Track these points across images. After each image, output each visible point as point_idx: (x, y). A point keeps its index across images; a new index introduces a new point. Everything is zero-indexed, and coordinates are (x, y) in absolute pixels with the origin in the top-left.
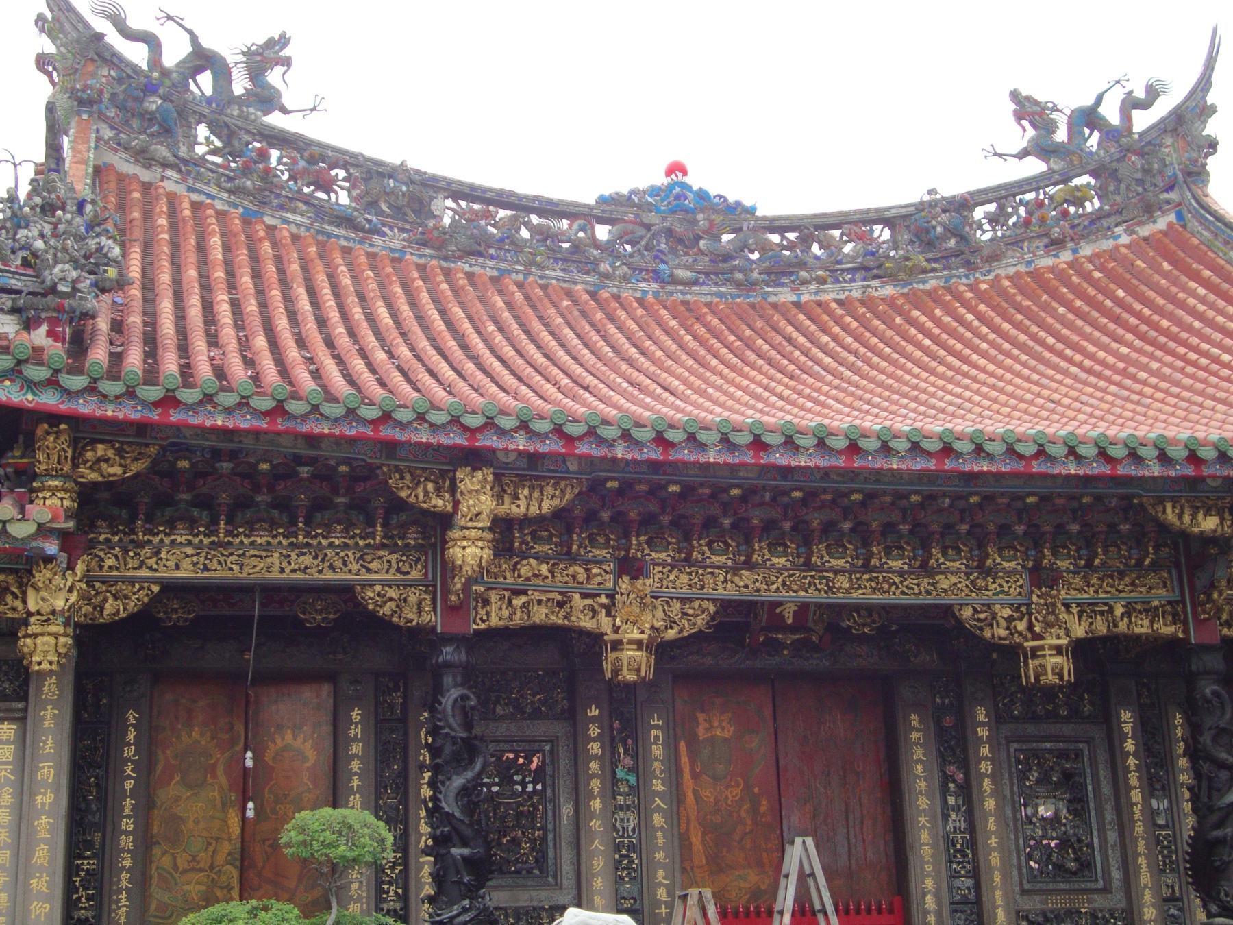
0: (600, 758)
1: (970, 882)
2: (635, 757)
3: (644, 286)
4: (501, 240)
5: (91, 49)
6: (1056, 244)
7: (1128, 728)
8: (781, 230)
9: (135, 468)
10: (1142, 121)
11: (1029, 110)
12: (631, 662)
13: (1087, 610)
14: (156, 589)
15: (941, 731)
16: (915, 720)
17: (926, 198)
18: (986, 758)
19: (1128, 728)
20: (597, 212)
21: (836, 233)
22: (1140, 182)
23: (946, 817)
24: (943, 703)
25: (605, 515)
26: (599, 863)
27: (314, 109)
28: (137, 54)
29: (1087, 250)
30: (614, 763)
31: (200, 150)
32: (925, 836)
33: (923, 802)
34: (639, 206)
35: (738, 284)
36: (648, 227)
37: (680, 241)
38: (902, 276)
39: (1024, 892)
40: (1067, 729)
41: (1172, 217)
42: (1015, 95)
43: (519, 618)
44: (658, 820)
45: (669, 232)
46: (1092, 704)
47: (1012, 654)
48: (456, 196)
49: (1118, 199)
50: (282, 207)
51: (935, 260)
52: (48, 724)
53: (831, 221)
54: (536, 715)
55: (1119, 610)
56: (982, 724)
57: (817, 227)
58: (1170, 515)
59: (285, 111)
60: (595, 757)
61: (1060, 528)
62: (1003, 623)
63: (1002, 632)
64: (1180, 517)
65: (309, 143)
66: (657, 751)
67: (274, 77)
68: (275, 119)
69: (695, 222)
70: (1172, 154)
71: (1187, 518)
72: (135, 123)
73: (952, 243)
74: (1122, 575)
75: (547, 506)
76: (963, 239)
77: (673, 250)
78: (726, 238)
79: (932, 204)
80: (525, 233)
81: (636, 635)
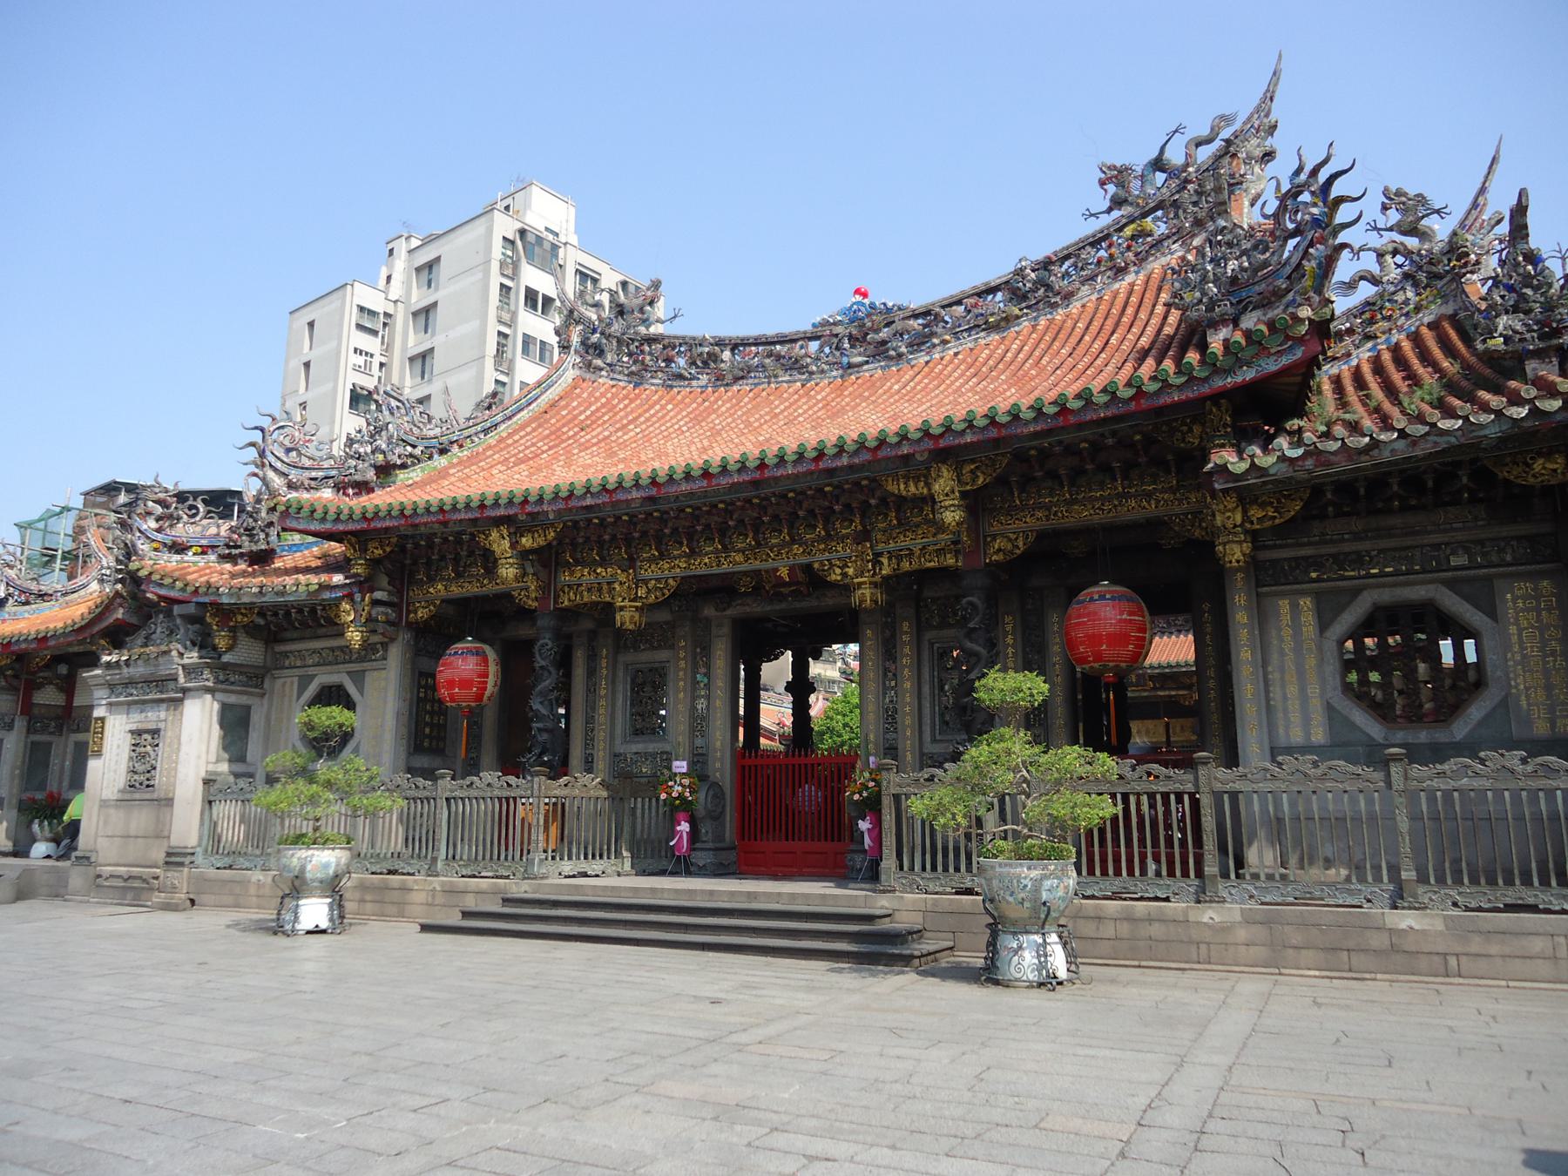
0: (685, 670)
2: (708, 668)
6: (1120, 271)
7: (1009, 628)
10: (1205, 154)
11: (1116, 176)
12: (627, 617)
13: (896, 556)
19: (1009, 628)
23: (885, 694)
30: (694, 673)
39: (934, 741)
44: (718, 703)
54: (659, 647)
57: (943, 307)
58: (892, 487)
62: (838, 571)
68: (655, 329)
74: (917, 526)
75: (541, 542)
76: (1048, 287)
81: (626, 603)
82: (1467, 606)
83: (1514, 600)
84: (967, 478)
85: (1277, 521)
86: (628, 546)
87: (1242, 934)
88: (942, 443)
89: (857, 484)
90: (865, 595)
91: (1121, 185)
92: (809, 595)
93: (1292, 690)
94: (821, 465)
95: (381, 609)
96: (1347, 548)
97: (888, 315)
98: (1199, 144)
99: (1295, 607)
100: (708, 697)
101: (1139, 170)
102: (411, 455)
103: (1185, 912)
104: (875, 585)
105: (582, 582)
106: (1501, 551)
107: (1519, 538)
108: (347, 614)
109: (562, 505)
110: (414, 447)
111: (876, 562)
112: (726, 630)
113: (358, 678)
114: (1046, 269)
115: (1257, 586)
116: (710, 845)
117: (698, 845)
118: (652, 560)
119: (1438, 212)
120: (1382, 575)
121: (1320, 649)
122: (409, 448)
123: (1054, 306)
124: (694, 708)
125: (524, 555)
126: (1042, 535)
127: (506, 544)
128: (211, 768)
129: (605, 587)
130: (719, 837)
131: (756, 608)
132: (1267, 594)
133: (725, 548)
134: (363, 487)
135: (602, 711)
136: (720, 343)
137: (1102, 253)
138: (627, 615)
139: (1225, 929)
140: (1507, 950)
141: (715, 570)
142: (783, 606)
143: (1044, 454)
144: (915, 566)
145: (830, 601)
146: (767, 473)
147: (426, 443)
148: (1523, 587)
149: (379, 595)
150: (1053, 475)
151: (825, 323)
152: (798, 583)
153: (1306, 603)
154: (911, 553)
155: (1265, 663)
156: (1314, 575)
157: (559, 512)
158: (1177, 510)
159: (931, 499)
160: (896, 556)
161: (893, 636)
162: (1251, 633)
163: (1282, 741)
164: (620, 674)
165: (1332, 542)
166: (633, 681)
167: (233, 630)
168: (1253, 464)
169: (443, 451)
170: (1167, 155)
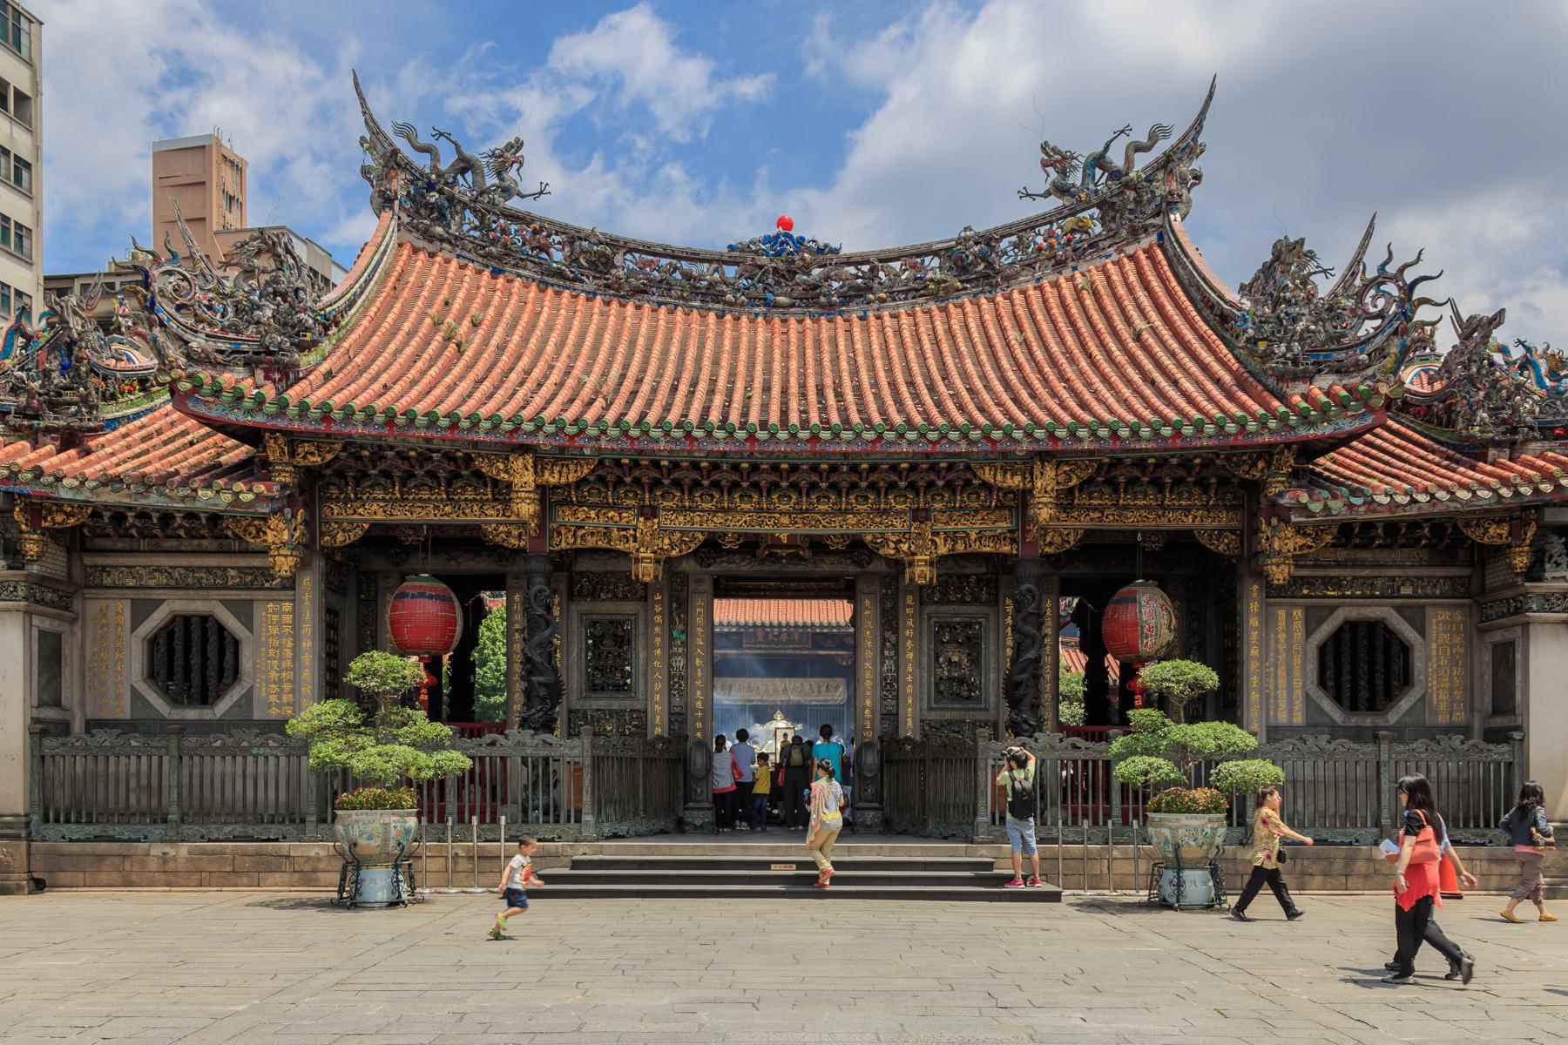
4: (661, 281)
8: (856, 264)
10: (1142, 161)
11: (1056, 160)
12: (646, 570)
13: (952, 537)
15: (884, 613)
16: (867, 602)
19: (1010, 609)
21: (896, 265)
22: (1131, 211)
23: (882, 664)
25: (628, 480)
27: (541, 193)
31: (466, 227)
32: (868, 675)
33: (869, 654)
34: (756, 252)
35: (822, 306)
36: (761, 267)
39: (930, 709)
40: (973, 609)
41: (1154, 238)
42: (1043, 149)
43: (578, 545)
46: (989, 594)
47: (898, 566)
48: (630, 251)
49: (1113, 226)
50: (516, 265)
52: (307, 603)
55: (973, 537)
57: (881, 261)
59: (523, 197)
61: (931, 484)
68: (514, 204)
69: (793, 262)
72: (422, 211)
73: (981, 267)
74: (977, 511)
76: (990, 265)
77: (778, 283)
78: (816, 272)
79: (966, 239)
80: (678, 275)
81: (649, 554)
90: (922, 572)
91: (1063, 173)
96: (1333, 572)
98: (1139, 148)
99: (1289, 615)
103: (1235, 853)
105: (584, 526)
107: (1445, 578)
112: (707, 586)
113: (244, 612)
114: (988, 244)
118: (681, 510)
120: (1353, 596)
126: (1088, 533)
128: (35, 713)
131: (742, 567)
136: (615, 244)
137: (1040, 240)
142: (776, 567)
148: (1444, 615)
151: (745, 249)
152: (797, 547)
153: (1298, 613)
154: (968, 535)
158: (1208, 523)
160: (952, 537)
161: (895, 607)
162: (1260, 635)
163: (1272, 723)
167: (45, 531)
170: (1110, 155)
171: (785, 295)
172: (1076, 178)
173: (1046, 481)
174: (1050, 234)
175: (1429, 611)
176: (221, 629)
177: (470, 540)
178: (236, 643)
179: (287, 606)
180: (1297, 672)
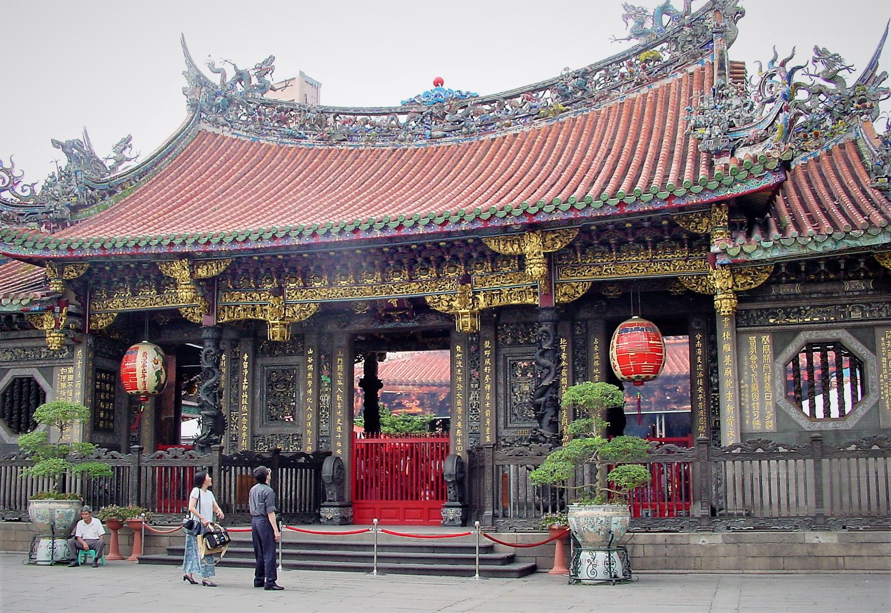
1: (477, 424)
3: (419, 142)
5: (200, 81)
7: (563, 348)
9: (82, 272)
11: (635, 14)
12: (276, 332)
14: (115, 315)
15: (471, 355)
17: (564, 73)
18: (488, 365)
20: (398, 110)
21: (519, 100)
24: (472, 340)
26: (310, 416)
27: (286, 86)
28: (216, 79)
29: (657, 85)
36: (422, 113)
37: (438, 117)
38: (551, 116)
39: (506, 427)
42: (625, 6)
45: (432, 114)
50: (267, 134)
51: (570, 105)
52: (79, 367)
53: (515, 93)
54: (291, 354)
56: (488, 349)
57: (506, 98)
58: (493, 246)
59: (273, 89)
60: (310, 371)
63: (446, 308)
64: (499, 245)
65: (277, 102)
66: (340, 367)
67: (268, 77)
68: (270, 96)
70: (711, 21)
71: (502, 247)
75: (214, 272)
82: (859, 344)
83: (886, 340)
84: (549, 243)
85: (753, 286)
86: (279, 278)
87: (722, 551)
88: (536, 219)
89: (465, 241)
92: (413, 317)
93: (756, 396)
94: (446, 229)
95: (72, 319)
97: (462, 100)
99: (759, 340)
100: (331, 394)
101: (651, 12)
102: (91, 197)
104: (473, 315)
105: (239, 305)
106: (880, 310)
108: (48, 324)
109: (237, 247)
110: (93, 189)
111: (475, 298)
113: (48, 373)
115: (737, 327)
116: (337, 504)
117: (326, 503)
119: (848, 68)
121: (773, 368)
122: (90, 191)
123: (590, 105)
124: (319, 401)
125: (197, 282)
127: (186, 273)
129: (258, 309)
130: (341, 498)
132: (743, 332)
133: (357, 284)
134: (61, 223)
135: (244, 402)
138: (277, 329)
139: (712, 548)
140: (871, 553)
141: (350, 298)
143: (601, 229)
144: (503, 303)
145: (432, 322)
146: (403, 232)
147: (101, 186)
149: (71, 308)
150: (605, 243)
152: (406, 309)
153: (766, 339)
155: (740, 378)
156: (772, 321)
157: (230, 253)
158: (688, 272)
159: (521, 258)
161: (477, 350)
163: (748, 430)
164: (258, 374)
165: (783, 300)
166: (268, 379)
168: (742, 250)
169: (111, 193)
171: (441, 130)
172: (648, 25)
173: (532, 246)
174: (631, 65)
175: (878, 331)
176: (38, 385)
177: (175, 319)
178: (45, 394)
179: (71, 370)
180: (768, 387)
